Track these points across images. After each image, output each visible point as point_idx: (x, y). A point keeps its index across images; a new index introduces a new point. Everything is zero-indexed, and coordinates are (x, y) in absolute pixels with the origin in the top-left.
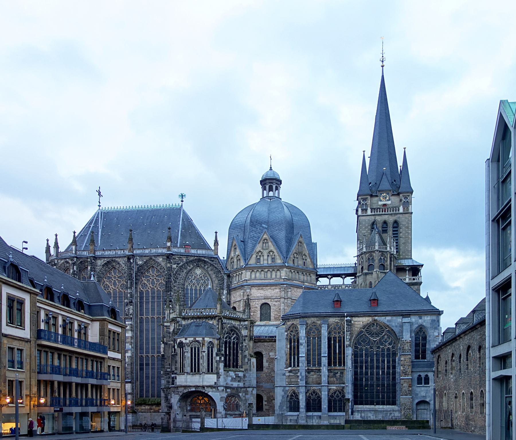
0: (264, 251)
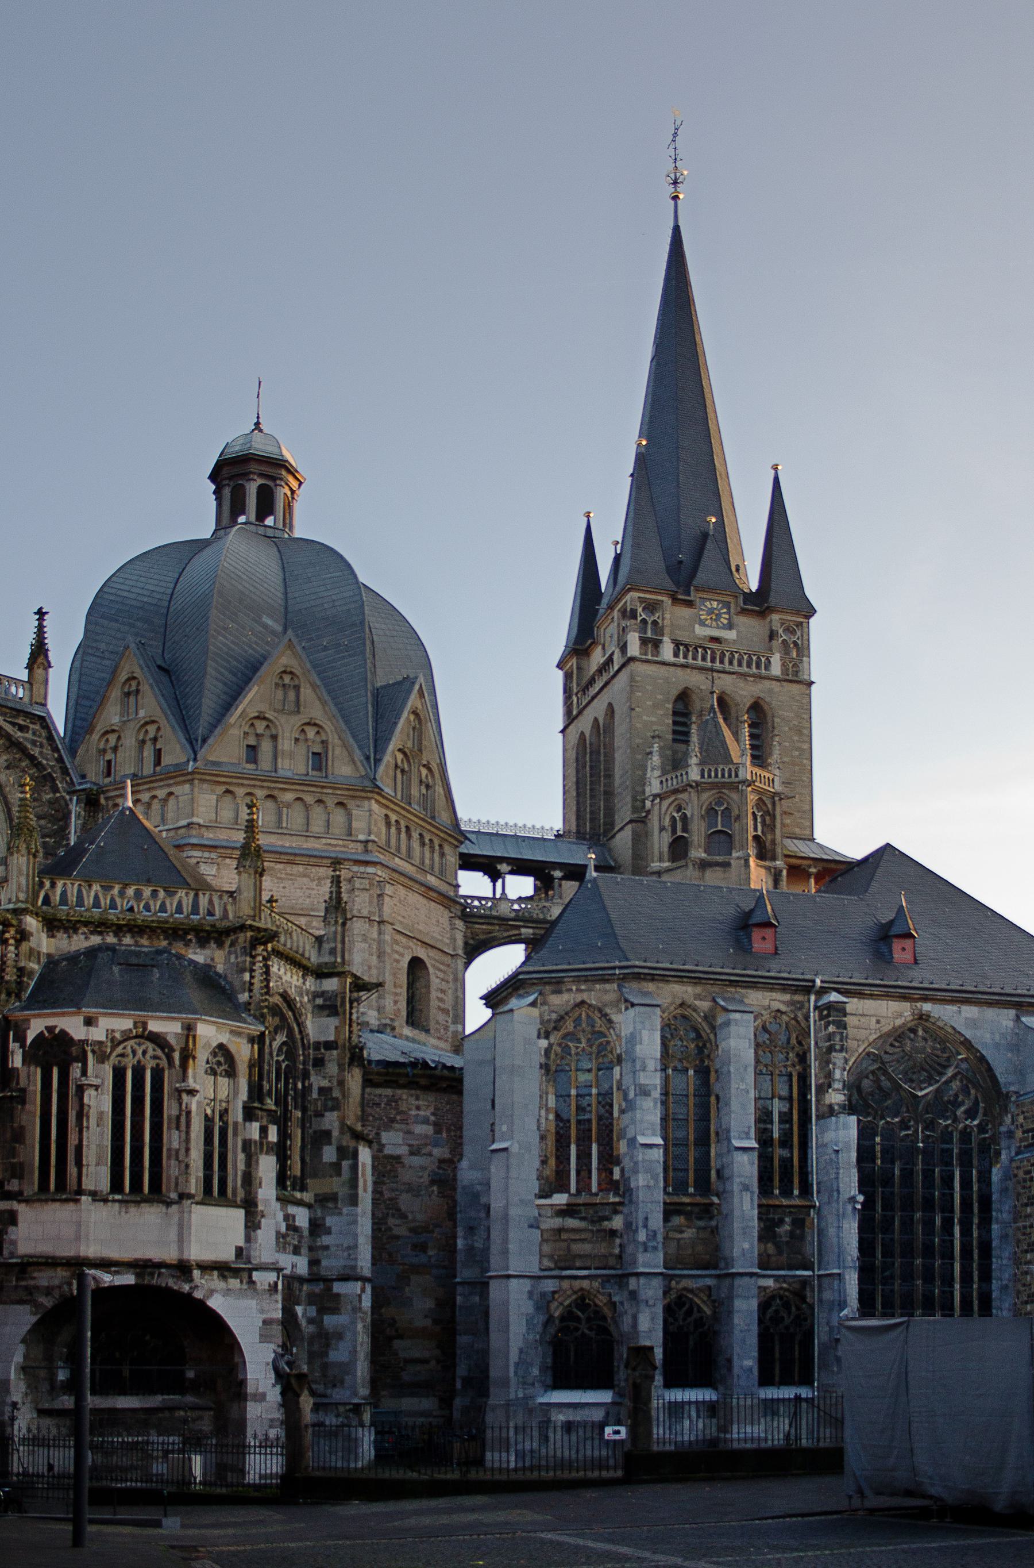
0: (283, 719)
